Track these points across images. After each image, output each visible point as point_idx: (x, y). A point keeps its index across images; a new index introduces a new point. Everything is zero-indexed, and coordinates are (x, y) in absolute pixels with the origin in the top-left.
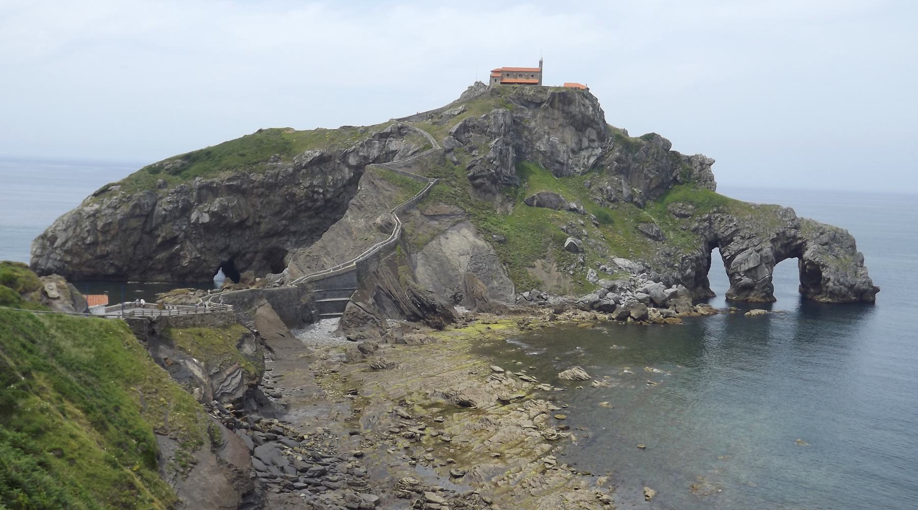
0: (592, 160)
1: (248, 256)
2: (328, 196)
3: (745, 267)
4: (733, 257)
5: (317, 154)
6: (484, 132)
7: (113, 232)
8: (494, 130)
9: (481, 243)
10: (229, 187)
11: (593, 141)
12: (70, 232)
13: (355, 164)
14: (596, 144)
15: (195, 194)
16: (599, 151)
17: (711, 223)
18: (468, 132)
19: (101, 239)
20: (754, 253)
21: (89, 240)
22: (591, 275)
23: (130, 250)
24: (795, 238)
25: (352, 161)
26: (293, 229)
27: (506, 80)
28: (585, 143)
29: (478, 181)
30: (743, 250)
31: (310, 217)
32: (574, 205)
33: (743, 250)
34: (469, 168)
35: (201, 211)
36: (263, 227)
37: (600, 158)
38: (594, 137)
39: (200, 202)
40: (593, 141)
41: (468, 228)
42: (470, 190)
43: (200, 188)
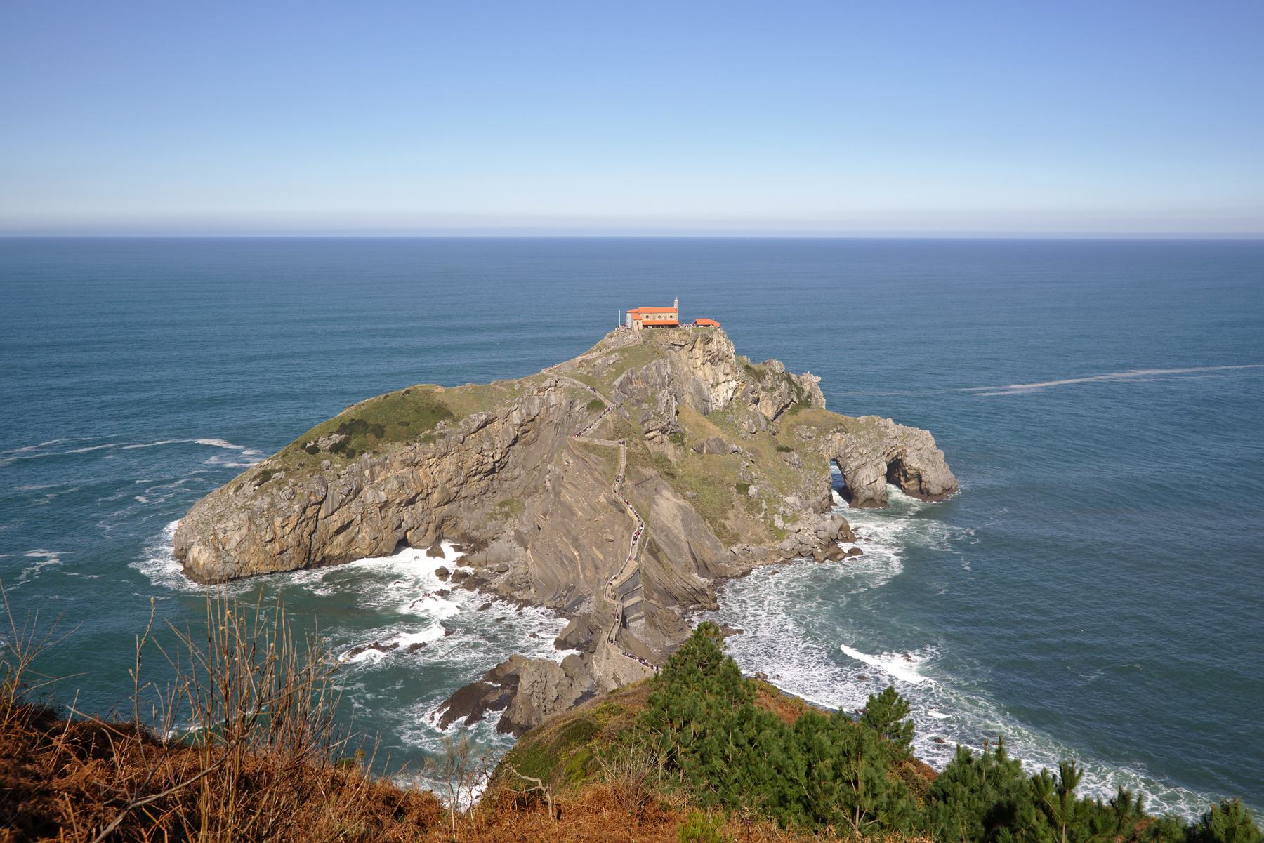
0: (730, 393)
1: (422, 528)
2: (497, 458)
3: (866, 482)
5: (484, 417)
7: (291, 526)
9: (682, 502)
10: (403, 461)
12: (244, 531)
14: (730, 377)
15: (367, 472)
16: (733, 384)
19: (279, 533)
21: (268, 537)
22: (779, 523)
23: (307, 541)
25: (516, 418)
26: (463, 494)
28: (722, 378)
29: (652, 434)
31: (480, 480)
32: (735, 448)
35: (376, 488)
36: (436, 497)
37: (736, 390)
39: (373, 480)
41: (666, 488)
42: (647, 442)
43: (373, 466)
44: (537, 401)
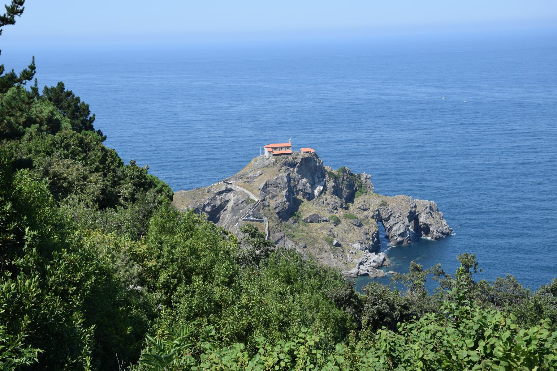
3: (399, 233)
4: (391, 228)
6: (278, 187)
8: (283, 185)
11: (320, 178)
13: (210, 210)
17: (379, 212)
18: (269, 187)
20: (402, 225)
24: (415, 212)
25: (208, 209)
27: (276, 152)
29: (281, 214)
30: (396, 224)
32: (325, 219)
33: (396, 224)
34: (276, 208)
38: (320, 176)
40: (320, 178)
44: (218, 198)
